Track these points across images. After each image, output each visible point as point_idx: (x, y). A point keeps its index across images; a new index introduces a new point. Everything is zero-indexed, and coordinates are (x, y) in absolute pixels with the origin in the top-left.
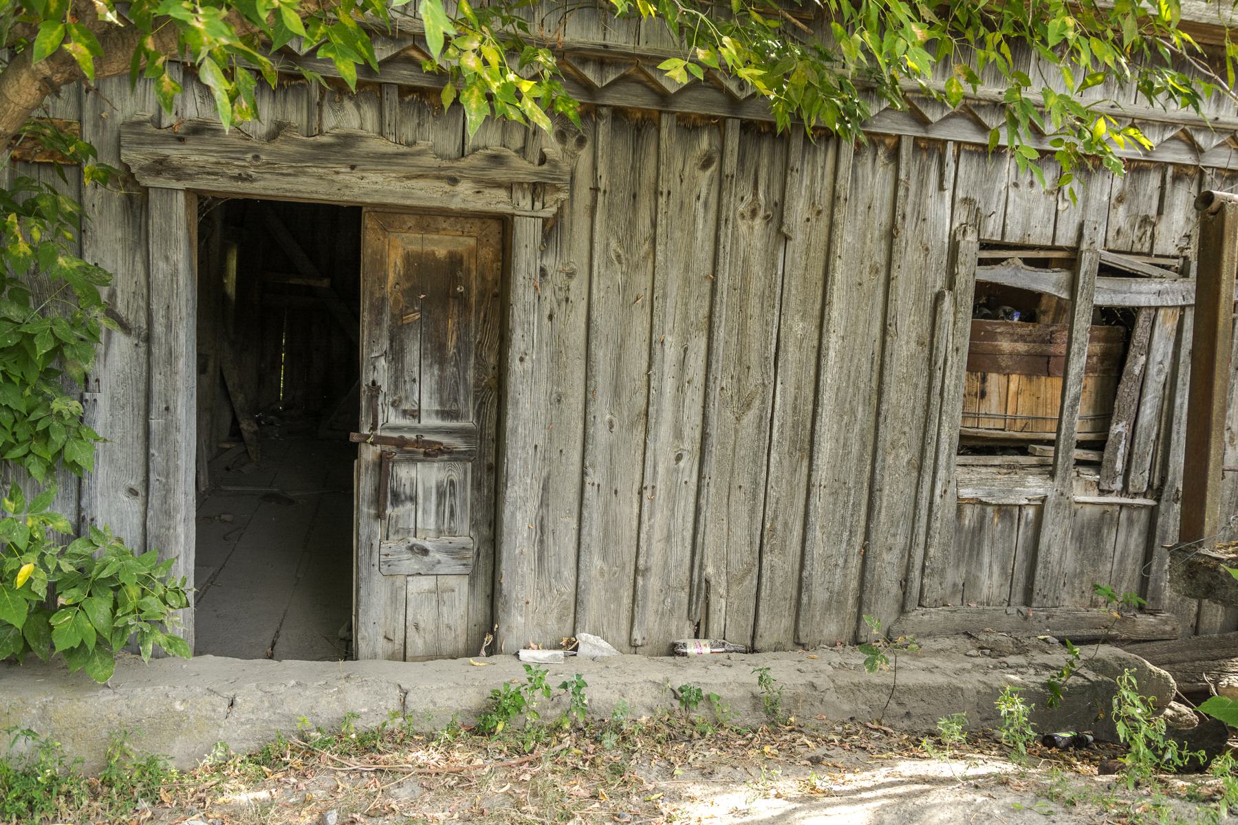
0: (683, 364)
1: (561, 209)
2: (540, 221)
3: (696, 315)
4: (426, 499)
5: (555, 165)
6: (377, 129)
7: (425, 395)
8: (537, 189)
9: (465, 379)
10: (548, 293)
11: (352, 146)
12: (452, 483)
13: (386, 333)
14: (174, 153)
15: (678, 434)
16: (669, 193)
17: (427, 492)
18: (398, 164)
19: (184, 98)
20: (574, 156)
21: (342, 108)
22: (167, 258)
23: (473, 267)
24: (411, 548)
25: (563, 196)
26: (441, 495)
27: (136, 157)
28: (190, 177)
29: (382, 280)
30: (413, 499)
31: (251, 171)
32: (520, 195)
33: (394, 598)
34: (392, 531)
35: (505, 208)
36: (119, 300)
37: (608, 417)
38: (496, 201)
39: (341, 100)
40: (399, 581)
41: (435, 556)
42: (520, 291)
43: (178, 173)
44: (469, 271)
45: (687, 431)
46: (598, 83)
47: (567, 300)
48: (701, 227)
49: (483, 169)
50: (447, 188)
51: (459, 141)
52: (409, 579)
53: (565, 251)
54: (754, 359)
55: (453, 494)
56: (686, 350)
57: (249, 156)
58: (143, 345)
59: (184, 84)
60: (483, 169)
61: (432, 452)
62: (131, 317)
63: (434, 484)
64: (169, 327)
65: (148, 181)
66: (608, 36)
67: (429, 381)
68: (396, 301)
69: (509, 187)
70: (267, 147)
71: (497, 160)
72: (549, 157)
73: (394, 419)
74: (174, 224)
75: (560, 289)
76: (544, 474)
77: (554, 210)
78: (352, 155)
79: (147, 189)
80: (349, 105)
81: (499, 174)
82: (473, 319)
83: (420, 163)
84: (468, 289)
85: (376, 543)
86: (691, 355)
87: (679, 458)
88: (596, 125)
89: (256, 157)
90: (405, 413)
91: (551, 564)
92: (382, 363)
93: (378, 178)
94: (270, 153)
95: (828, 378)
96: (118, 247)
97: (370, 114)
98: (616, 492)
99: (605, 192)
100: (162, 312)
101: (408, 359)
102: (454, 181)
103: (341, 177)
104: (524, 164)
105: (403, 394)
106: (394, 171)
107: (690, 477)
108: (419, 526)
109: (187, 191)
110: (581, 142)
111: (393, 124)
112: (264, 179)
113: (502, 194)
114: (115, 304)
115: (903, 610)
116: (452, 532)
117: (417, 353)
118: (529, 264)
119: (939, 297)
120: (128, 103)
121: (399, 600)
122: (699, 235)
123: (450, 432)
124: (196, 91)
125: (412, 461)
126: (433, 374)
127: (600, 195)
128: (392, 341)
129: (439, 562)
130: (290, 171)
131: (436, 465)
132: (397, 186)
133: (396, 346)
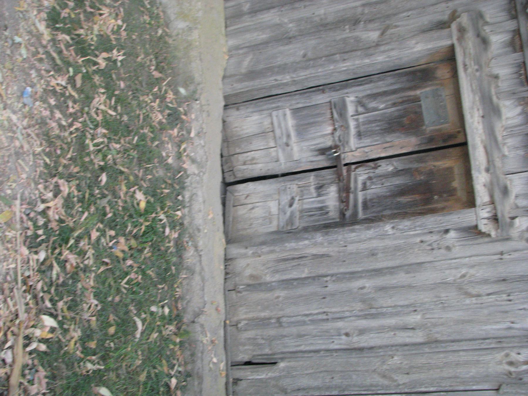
0: (405, 328)
1: (484, 233)
3: (437, 333)
4: (320, 202)
5: (511, 225)
7: (376, 190)
8: (495, 219)
9: (385, 210)
12: (327, 213)
13: (407, 167)
14: (470, 35)
15: (362, 332)
16: (510, 300)
17: (322, 202)
21: (516, 106)
22: (417, 43)
23: (450, 203)
24: (293, 199)
25: (493, 234)
26: (321, 209)
27: (464, 20)
29: (436, 160)
30: (319, 195)
34: (302, 188)
35: (479, 201)
37: (367, 285)
38: (482, 195)
39: (522, 105)
40: (276, 197)
43: (461, 39)
45: (364, 337)
47: (433, 249)
48: (494, 327)
49: (498, 184)
51: (515, 171)
52: (277, 201)
53: (462, 243)
54: (414, 377)
55: (322, 215)
56: (413, 329)
58: (374, 44)
59: (508, 32)
60: (498, 184)
61: (344, 200)
62: (386, 37)
63: (327, 203)
64: (384, 52)
65: (454, 26)
69: (492, 202)
71: (505, 191)
72: (514, 220)
73: (361, 179)
74: (435, 42)
76: (332, 254)
79: (449, 27)
80: (519, 109)
81: (498, 195)
82: (420, 208)
84: (437, 202)
85: (296, 182)
86: (410, 333)
87: (347, 335)
89: (477, 70)
90: (364, 184)
91: (282, 266)
92: (390, 168)
98: (324, 298)
99: (501, 259)
101: (395, 179)
102: (487, 170)
105: (374, 180)
107: (337, 344)
108: (305, 201)
114: (392, 28)
116: (301, 217)
117: (398, 182)
122: (489, 327)
125: (339, 191)
126: (387, 192)
127: (499, 256)
129: (285, 214)
131: (337, 204)
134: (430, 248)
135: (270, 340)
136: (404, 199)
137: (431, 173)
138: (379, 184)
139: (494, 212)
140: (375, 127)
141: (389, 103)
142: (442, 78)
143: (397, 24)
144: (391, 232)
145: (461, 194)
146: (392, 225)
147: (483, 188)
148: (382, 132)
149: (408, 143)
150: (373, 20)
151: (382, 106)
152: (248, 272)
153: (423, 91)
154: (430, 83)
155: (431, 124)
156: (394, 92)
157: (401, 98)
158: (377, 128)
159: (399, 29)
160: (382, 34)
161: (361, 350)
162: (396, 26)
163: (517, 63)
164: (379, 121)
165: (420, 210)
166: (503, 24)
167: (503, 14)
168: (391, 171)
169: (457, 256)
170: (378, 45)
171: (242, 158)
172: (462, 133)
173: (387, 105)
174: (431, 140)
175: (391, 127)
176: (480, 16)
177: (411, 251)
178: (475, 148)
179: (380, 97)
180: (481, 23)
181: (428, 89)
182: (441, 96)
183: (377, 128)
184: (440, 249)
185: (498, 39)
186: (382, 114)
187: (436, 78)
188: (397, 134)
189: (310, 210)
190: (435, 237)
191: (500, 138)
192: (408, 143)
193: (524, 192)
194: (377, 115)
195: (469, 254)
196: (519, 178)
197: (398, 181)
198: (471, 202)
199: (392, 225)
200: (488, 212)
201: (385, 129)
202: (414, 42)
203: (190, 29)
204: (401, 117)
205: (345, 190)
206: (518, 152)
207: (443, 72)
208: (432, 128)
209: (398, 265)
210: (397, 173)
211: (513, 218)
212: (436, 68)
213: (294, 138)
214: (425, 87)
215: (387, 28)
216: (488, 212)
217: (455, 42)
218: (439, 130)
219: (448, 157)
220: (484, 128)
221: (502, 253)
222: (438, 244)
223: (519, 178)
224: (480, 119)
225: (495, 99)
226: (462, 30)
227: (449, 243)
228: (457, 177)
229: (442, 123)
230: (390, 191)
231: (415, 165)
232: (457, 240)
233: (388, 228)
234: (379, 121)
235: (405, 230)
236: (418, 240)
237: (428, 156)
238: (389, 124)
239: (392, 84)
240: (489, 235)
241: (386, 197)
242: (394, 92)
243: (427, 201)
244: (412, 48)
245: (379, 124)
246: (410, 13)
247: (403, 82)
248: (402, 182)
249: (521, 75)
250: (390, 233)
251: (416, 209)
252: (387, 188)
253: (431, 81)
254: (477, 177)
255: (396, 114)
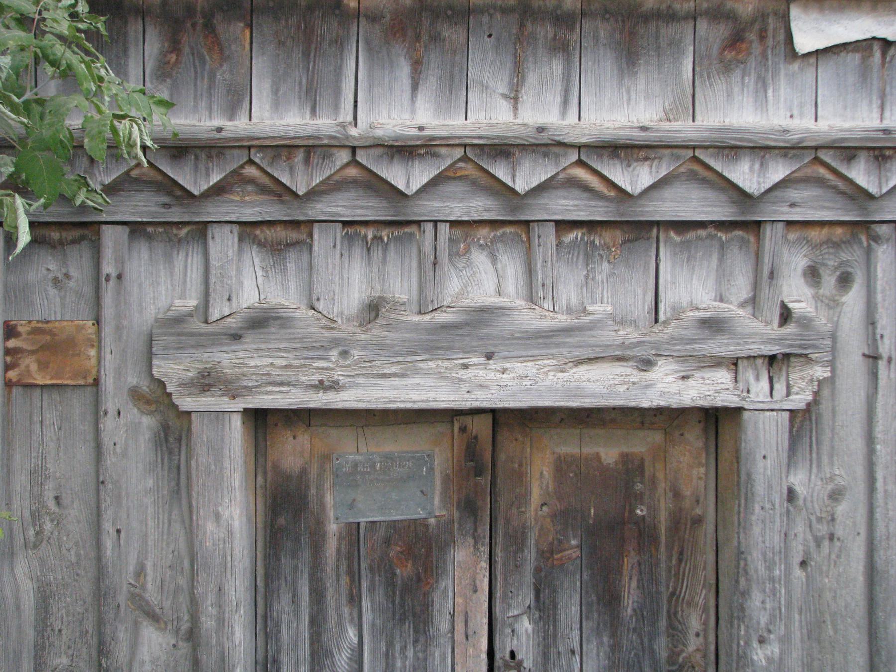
1: (816, 394)
2: (786, 415)
5: (806, 322)
6: (522, 291)
9: (652, 652)
10: (800, 528)
11: (486, 323)
13: (528, 578)
14: (226, 359)
18: (557, 345)
19: (239, 271)
20: (833, 304)
21: (469, 264)
22: (217, 516)
23: (660, 475)
25: (821, 372)
27: (172, 369)
28: (249, 390)
29: (522, 499)
31: (336, 375)
32: (750, 376)
35: (728, 399)
36: (149, 579)
39: (468, 251)
42: (756, 529)
44: (653, 481)
46: (873, 189)
47: (832, 537)
50: (636, 376)
53: (825, 460)
57: (334, 354)
62: (167, 604)
64: (221, 621)
65: (186, 403)
66: (887, 114)
68: (542, 531)
69: (734, 363)
70: (362, 337)
71: (713, 325)
74: (226, 464)
75: (820, 520)
77: (808, 397)
78: (489, 337)
80: (480, 258)
81: (720, 347)
83: (592, 341)
84: (653, 510)
88: (869, 252)
89: (345, 354)
92: (526, 625)
93: (529, 368)
94: (365, 347)
96: (149, 500)
97: (511, 266)
99: (889, 360)
100: (210, 599)
101: (562, 617)
102: (646, 364)
103: (472, 372)
104: (757, 326)
106: (552, 357)
109: (246, 412)
110: (845, 281)
111: (548, 283)
112: (358, 386)
113: (723, 376)
114: (144, 587)
117: (575, 610)
118: (770, 487)
120: (162, 289)
124: (257, 261)
126: (601, 643)
127: (882, 365)
128: (537, 593)
130: (394, 369)
132: (556, 380)
133: (545, 594)
134: (826, 543)
137: (565, 517)
138: (570, 659)
139: (759, 362)
140: (404, 657)
141: (346, 610)
142: (307, 455)
143: (131, 569)
144: (774, 649)
145: (639, 444)
146: (755, 644)
147: (690, 383)
148: (422, 639)
150: (101, 643)
151: (352, 633)
153: (331, 514)
154: (313, 491)
155: (424, 502)
156: (318, 595)
157: (338, 576)
158: (410, 653)
159: (149, 565)
160: (154, 617)
162: (140, 572)
163: (342, 242)
164: (390, 645)
165: (670, 557)
166: (214, 263)
167: (179, 260)
168: (536, 623)
169: (860, 471)
170: (193, 635)
172: (468, 420)
173: (352, 621)
174: (469, 507)
175: (414, 615)
176: (175, 322)
177: (828, 596)
178: (577, 392)
179: (324, 638)
180: (196, 325)
181: (329, 499)
182: (356, 465)
183: (410, 653)
184: (833, 519)
185: (253, 283)
186: (373, 635)
187: (304, 472)
188: (436, 597)
190: (800, 528)
191: (563, 320)
192: (465, 568)
193: (711, 282)
194: (374, 652)
195: (857, 444)
196: (673, 283)
197: (570, 608)
198: (717, 421)
199: (755, 644)
200: (757, 379)
201: (416, 631)
202: (210, 526)
204: (390, 583)
206: (599, 278)
207: (292, 450)
208: (436, 501)
209: (865, 638)
210: (545, 609)
211: (786, 315)
212: (276, 467)
214: (322, 505)
215: (138, 601)
216: (757, 379)
217: (240, 404)
218: (446, 480)
219: (520, 465)
220: (524, 358)
221: (873, 358)
222: (820, 520)
223: (673, 283)
224: (494, 364)
225: (441, 317)
226: (206, 382)
227: (821, 490)
228: (588, 450)
229: (431, 469)
230: (599, 635)
231: (530, 556)
232: (815, 470)
234: (390, 645)
235: (774, 610)
236: (798, 573)
237: (507, 521)
238: (402, 620)
239: (295, 600)
240: (820, 383)
241: (615, 647)
242: (318, 595)
243: (646, 535)
244: (230, 531)
245: (398, 647)
246: (108, 526)
247: (296, 568)
248: (577, 598)
249: (378, 239)
250: (776, 650)
251: (663, 566)
252: (588, 641)
253: (307, 487)
254: (662, 394)
255: (380, 593)
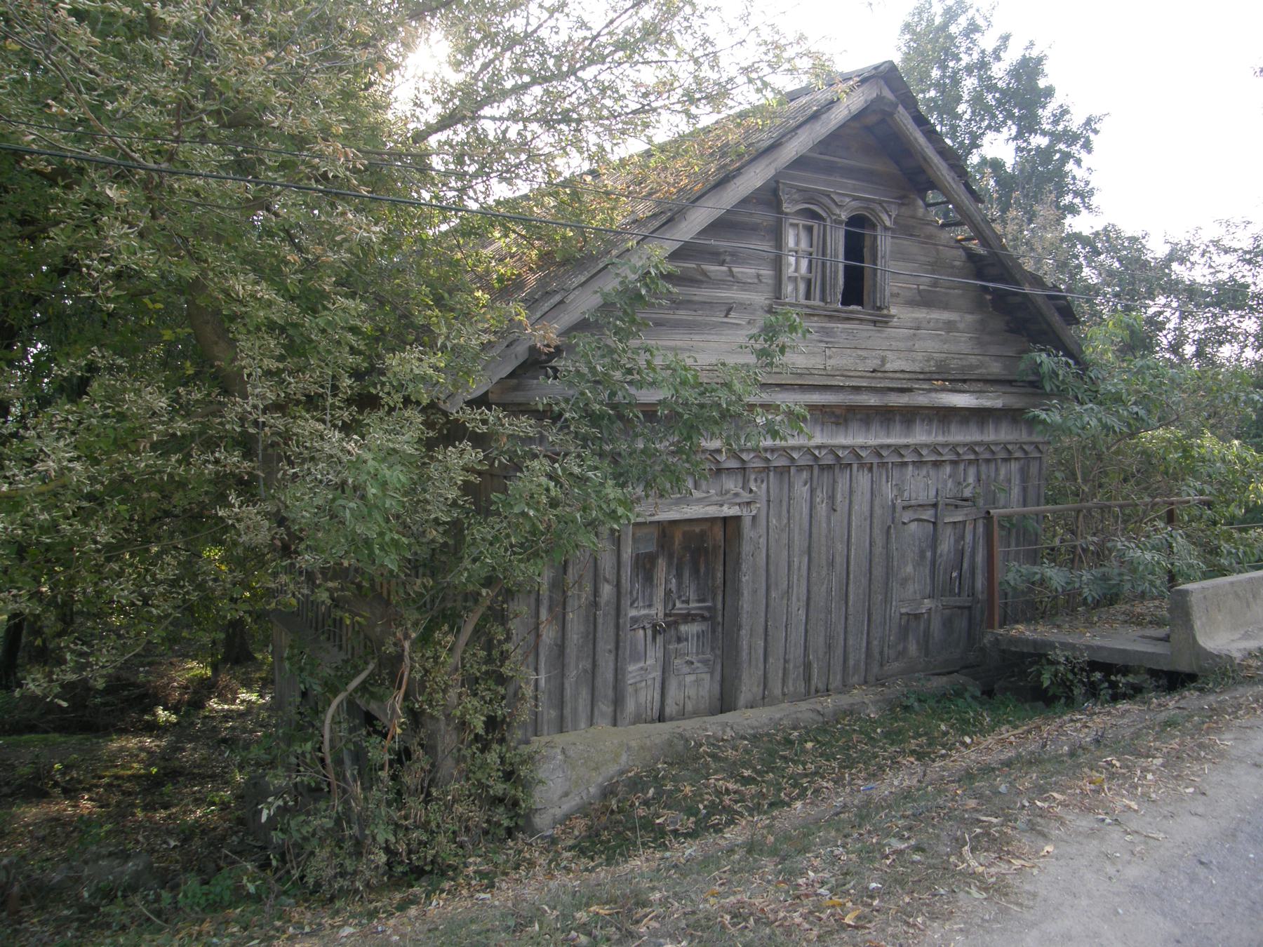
0: (799, 568)
15: (798, 600)
30: (687, 640)
33: (680, 684)
41: (697, 664)
67: (693, 587)
69: (739, 505)
71: (736, 495)
81: (738, 500)
90: (683, 602)
95: (852, 568)
102: (722, 505)
115: (882, 665)
116: (703, 653)
119: (889, 527)
121: (681, 686)
123: (700, 608)
125: (686, 622)
135: (795, 667)
136: (702, 570)
145: (705, 527)
149: (662, 563)
152: (755, 689)
161: (808, 599)
171: (649, 712)
189: (698, 645)
197: (686, 574)
203: (629, 748)
205: (688, 618)
210: (679, 576)
213: (642, 664)
233: (744, 579)
